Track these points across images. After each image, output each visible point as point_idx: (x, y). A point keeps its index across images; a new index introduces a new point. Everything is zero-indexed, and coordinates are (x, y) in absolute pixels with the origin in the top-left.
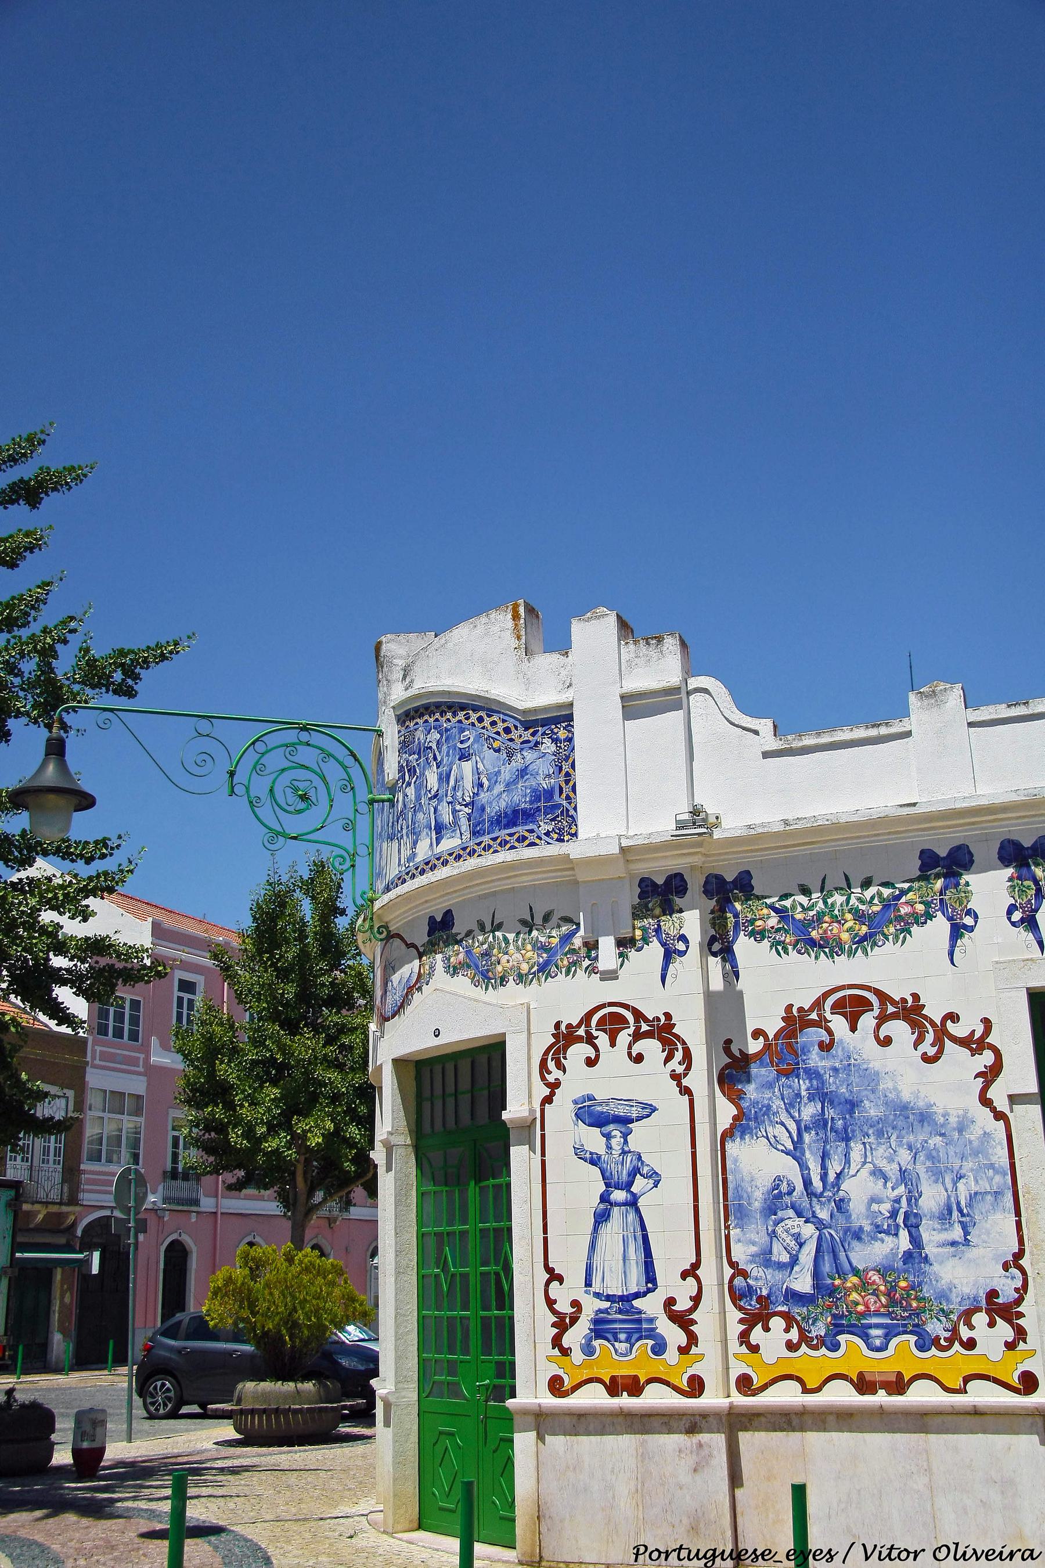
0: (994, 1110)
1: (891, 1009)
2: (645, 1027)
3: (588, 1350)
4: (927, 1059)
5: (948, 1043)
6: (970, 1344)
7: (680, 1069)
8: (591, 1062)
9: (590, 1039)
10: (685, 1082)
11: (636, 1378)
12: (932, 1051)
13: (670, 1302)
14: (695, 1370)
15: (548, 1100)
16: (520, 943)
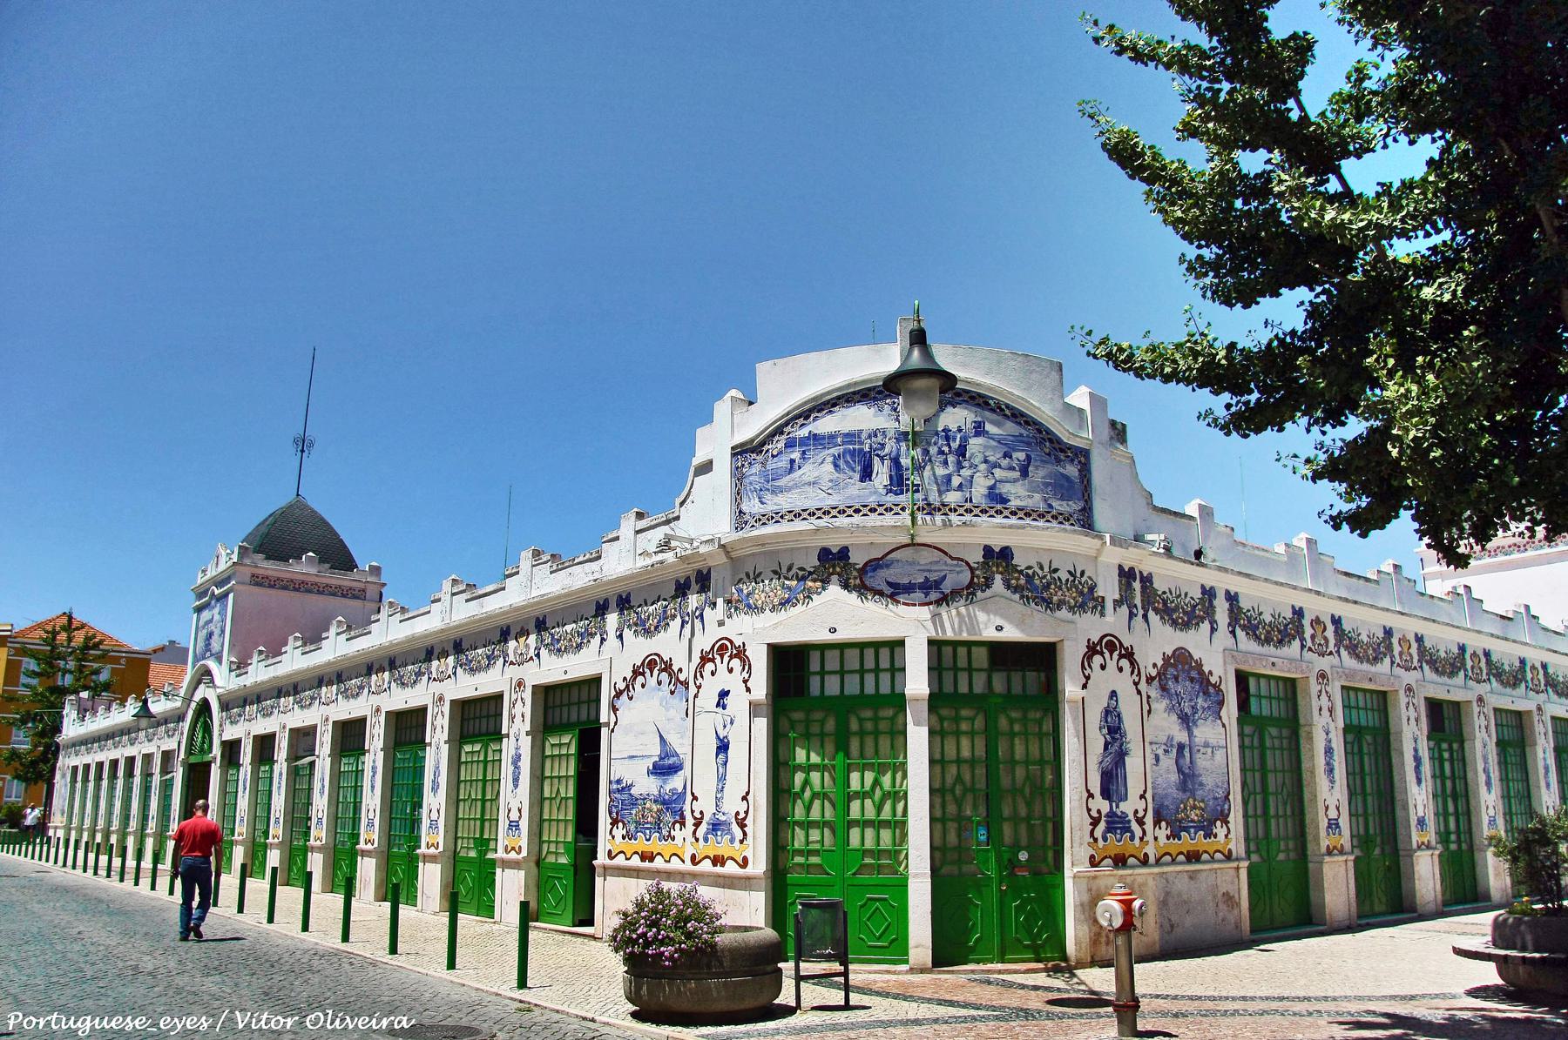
2: (1123, 652)
6: (1215, 836)
9: (1102, 654)
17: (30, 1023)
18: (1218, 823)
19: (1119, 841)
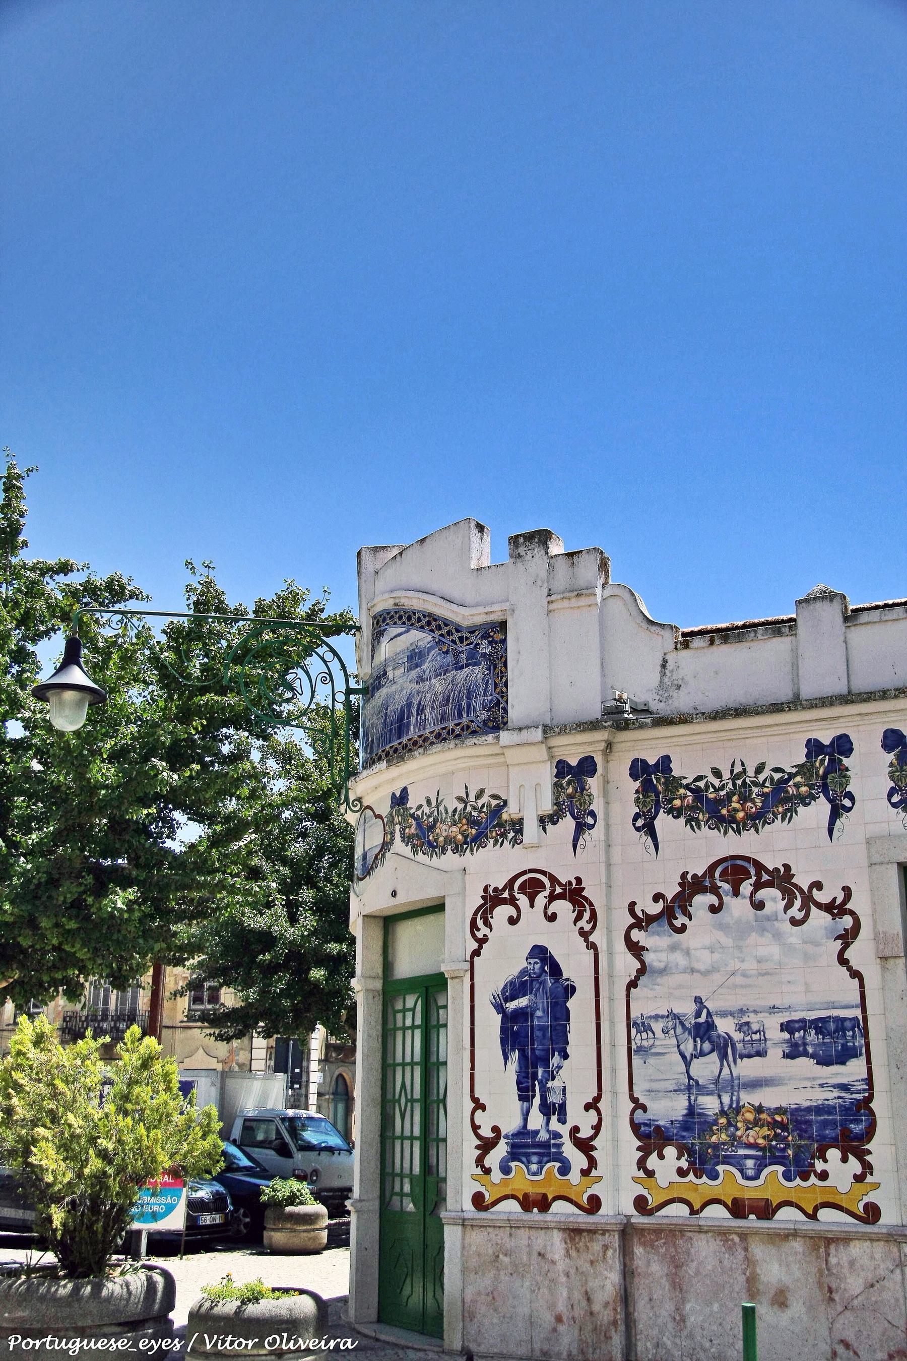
0: (849, 969)
1: (765, 877)
2: (558, 890)
3: (505, 1170)
4: (795, 922)
5: (813, 908)
7: (587, 927)
8: (513, 921)
9: (513, 901)
10: (591, 939)
11: (545, 1196)
12: (799, 916)
13: (576, 1129)
14: (595, 1190)
15: (476, 953)
16: (456, 817)
17: (27, 1344)
18: (834, 1154)
19: (534, 1174)
